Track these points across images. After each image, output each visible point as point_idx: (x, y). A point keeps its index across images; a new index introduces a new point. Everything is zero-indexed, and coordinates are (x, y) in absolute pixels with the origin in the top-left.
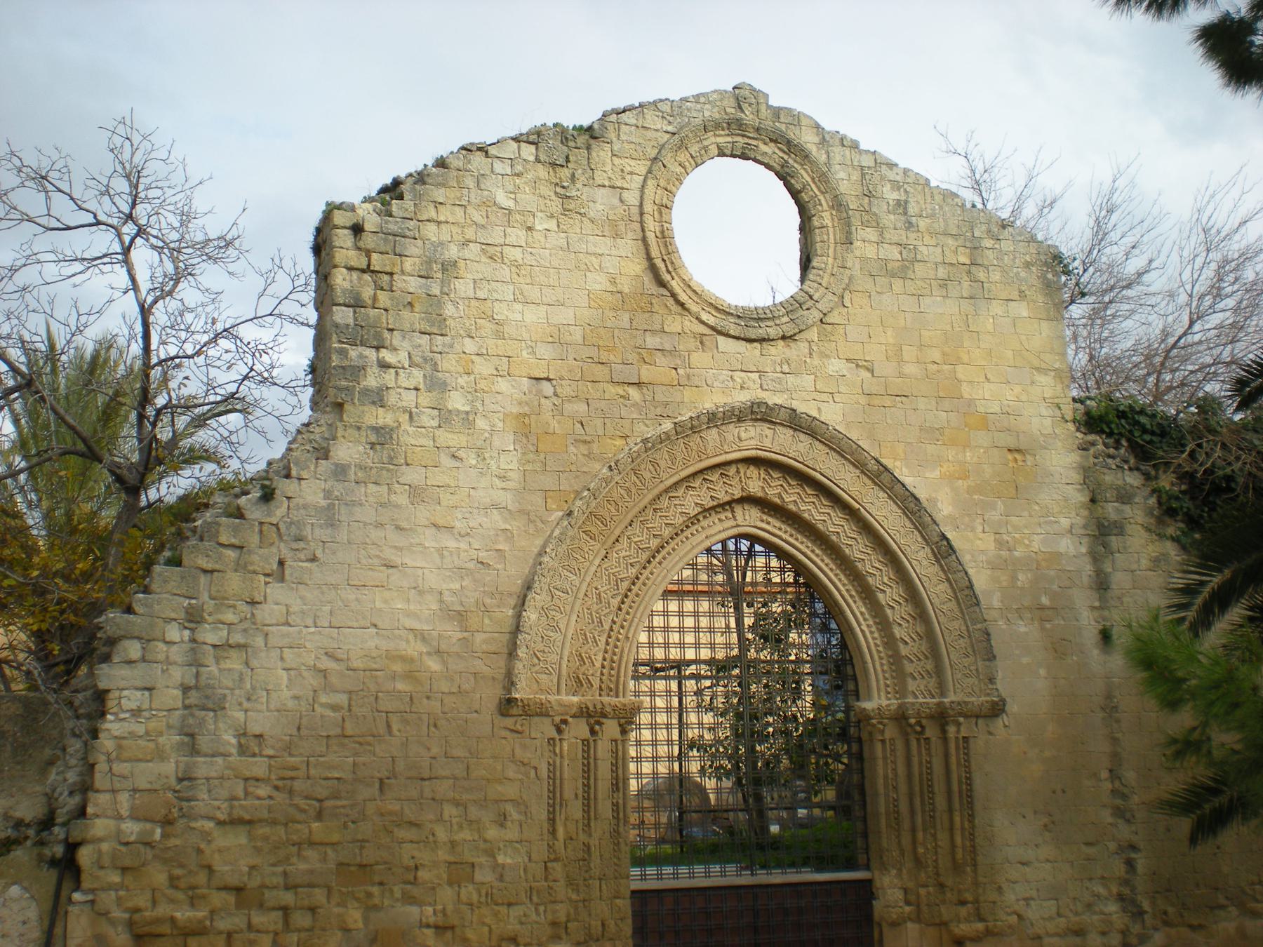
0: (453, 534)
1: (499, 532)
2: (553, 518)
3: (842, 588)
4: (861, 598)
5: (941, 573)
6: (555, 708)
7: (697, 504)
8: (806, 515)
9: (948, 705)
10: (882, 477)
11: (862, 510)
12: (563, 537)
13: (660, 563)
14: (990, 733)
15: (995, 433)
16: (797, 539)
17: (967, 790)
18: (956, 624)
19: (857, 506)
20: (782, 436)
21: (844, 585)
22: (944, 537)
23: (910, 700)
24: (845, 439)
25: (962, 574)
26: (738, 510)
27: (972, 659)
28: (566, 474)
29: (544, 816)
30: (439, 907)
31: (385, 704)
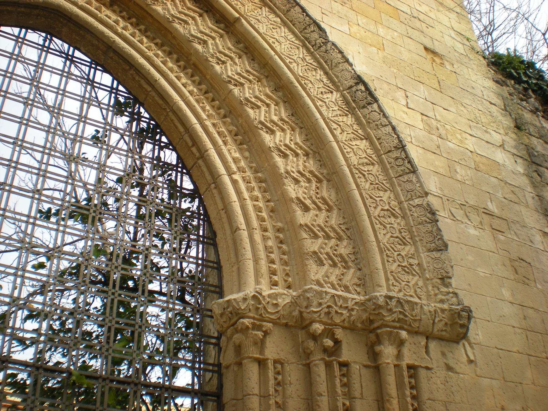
9: (381, 301)
11: (243, 21)
14: (449, 368)
19: (237, 15)
22: (359, 80)
25: (389, 129)
27: (409, 249)
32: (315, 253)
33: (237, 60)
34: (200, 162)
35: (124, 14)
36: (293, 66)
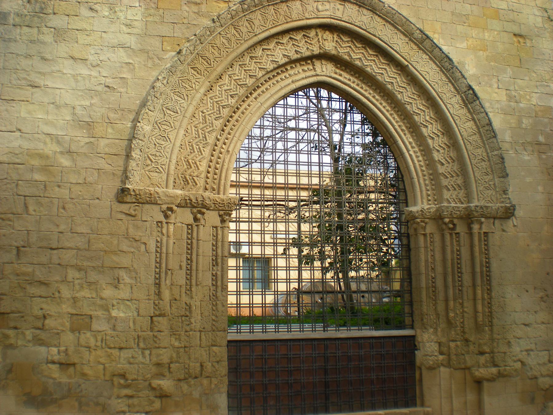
0: (87, 65)
1: (124, 65)
2: (167, 56)
3: (395, 124)
4: (409, 131)
5: (468, 114)
6: (162, 198)
7: (284, 55)
8: (368, 69)
9: (473, 208)
10: (425, 43)
11: (410, 66)
12: (173, 70)
13: (256, 98)
14: (504, 231)
15: (505, 23)
16: (362, 88)
17: (487, 271)
18: (479, 151)
19: (406, 63)
20: (350, 10)
21: (397, 122)
22: (470, 88)
23: (446, 204)
24: (397, 14)
25: (484, 114)
26: (318, 64)
27: (490, 177)
28: (179, 25)
29: (151, 281)
30: (63, 348)
31: (24, 190)
32: (446, 186)
33: (408, 90)
34: (394, 145)
36: (436, 87)
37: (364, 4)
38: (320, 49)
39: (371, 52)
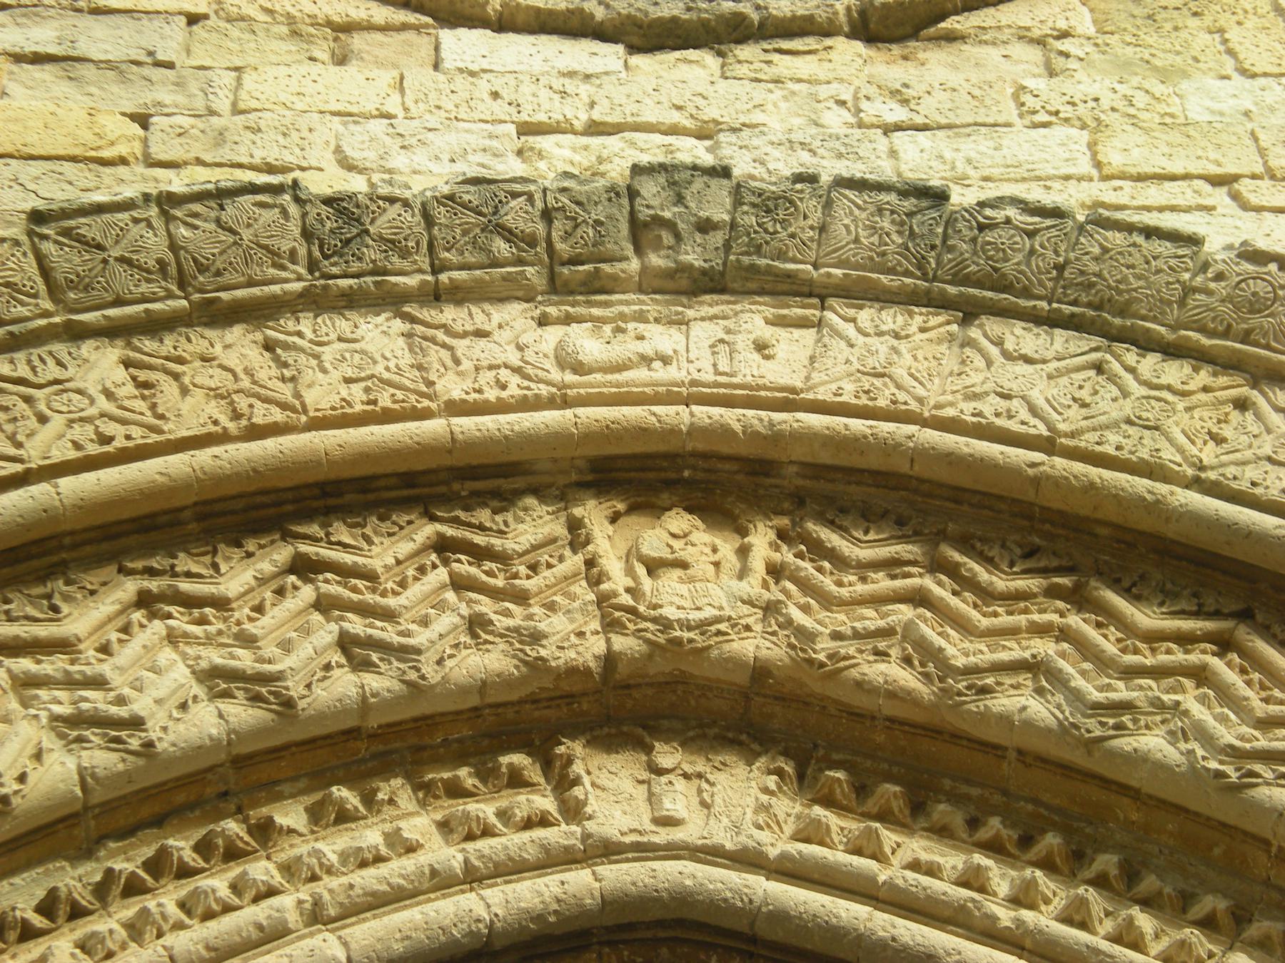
20: (882, 346)
35: (994, 825)
37: (1003, 285)
38: (610, 625)
39: (1145, 617)
